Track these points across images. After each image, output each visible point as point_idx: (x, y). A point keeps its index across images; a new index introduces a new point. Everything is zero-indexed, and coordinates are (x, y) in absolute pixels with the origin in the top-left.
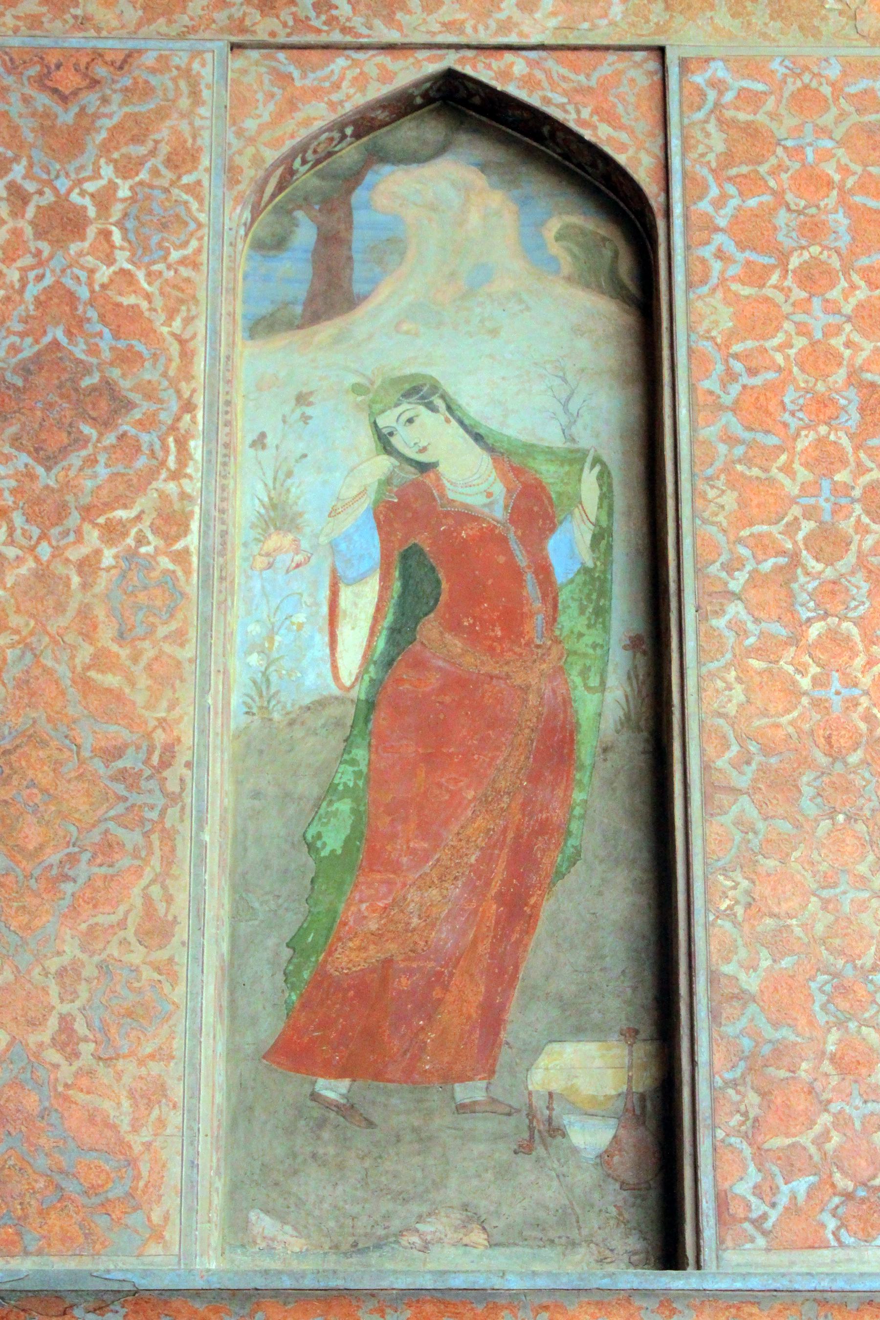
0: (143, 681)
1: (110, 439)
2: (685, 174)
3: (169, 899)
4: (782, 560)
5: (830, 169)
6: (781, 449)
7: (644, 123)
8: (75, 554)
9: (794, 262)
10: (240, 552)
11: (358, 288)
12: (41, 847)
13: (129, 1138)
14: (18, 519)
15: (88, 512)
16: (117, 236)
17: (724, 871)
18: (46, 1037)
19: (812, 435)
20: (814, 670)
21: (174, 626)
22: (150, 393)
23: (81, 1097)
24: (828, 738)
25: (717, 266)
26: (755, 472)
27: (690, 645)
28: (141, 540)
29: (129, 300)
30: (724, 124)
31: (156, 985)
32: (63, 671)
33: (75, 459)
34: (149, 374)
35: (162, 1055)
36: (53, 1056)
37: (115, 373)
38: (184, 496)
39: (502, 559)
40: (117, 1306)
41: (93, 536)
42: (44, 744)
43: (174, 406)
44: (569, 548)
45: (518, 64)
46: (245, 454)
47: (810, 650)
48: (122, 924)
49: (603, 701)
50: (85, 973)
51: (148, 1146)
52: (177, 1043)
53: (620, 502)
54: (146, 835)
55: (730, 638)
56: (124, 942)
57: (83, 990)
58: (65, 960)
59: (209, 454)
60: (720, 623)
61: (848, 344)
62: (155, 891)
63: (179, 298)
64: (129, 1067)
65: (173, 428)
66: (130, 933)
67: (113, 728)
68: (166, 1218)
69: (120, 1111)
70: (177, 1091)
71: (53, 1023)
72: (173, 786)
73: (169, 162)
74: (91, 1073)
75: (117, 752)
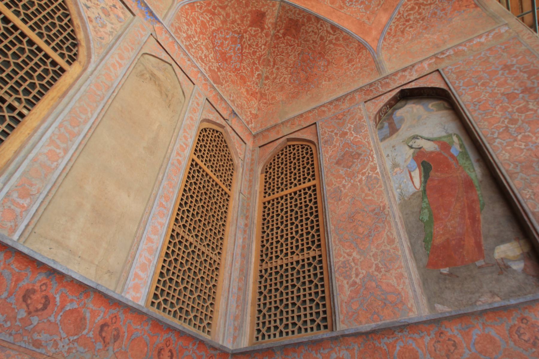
0: (376, 196)
1: (359, 160)
2: (451, 83)
3: (392, 234)
4: (504, 128)
5: (479, 69)
6: (493, 111)
7: (440, 79)
8: (357, 180)
9: (479, 84)
10: (390, 174)
11: (398, 128)
12: (363, 232)
13: (398, 288)
14: (346, 178)
15: (358, 173)
16: (353, 132)
17: (524, 190)
18: (373, 270)
19: (499, 107)
20: (523, 144)
21: (379, 185)
22: (364, 151)
23: (384, 281)
24: (535, 155)
25: (464, 92)
26: (489, 117)
27: (490, 150)
28: (369, 173)
29: (357, 140)
30: (454, 73)
31: (394, 253)
32: (360, 199)
33: (354, 166)
34: (364, 149)
35: (400, 267)
36: (376, 273)
37: (358, 151)
38: (374, 164)
39: (442, 157)
40: (405, 330)
41: (360, 176)
42: (359, 213)
43: (369, 151)
44: (456, 149)
45: (413, 83)
46: (386, 159)
47: (520, 141)
48: (384, 242)
49: (476, 173)
50: (378, 254)
51: (402, 289)
52: (403, 264)
53: (463, 138)
54: (384, 223)
55: (499, 146)
56: (385, 245)
57: (379, 257)
58: (373, 252)
59: (377, 156)
60: (496, 144)
61: (498, 90)
62: (389, 233)
63: (365, 136)
64: (393, 271)
65: (370, 155)
66: (386, 243)
67: (372, 206)
68: (412, 305)
69: (394, 282)
70: (406, 274)
71: (374, 266)
72: (387, 213)
73: (359, 120)
74: (385, 275)
75: (374, 210)
